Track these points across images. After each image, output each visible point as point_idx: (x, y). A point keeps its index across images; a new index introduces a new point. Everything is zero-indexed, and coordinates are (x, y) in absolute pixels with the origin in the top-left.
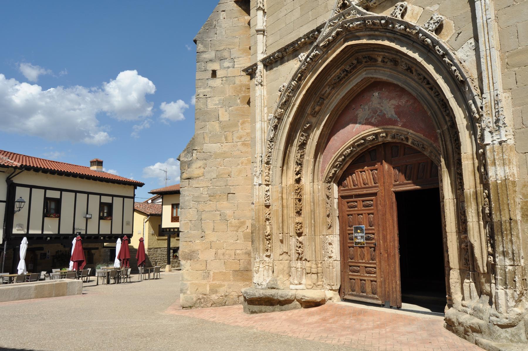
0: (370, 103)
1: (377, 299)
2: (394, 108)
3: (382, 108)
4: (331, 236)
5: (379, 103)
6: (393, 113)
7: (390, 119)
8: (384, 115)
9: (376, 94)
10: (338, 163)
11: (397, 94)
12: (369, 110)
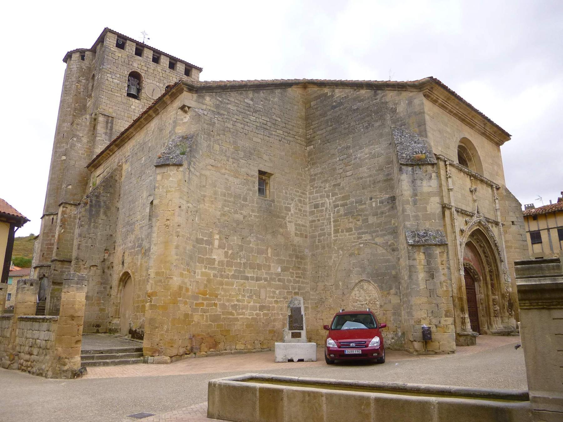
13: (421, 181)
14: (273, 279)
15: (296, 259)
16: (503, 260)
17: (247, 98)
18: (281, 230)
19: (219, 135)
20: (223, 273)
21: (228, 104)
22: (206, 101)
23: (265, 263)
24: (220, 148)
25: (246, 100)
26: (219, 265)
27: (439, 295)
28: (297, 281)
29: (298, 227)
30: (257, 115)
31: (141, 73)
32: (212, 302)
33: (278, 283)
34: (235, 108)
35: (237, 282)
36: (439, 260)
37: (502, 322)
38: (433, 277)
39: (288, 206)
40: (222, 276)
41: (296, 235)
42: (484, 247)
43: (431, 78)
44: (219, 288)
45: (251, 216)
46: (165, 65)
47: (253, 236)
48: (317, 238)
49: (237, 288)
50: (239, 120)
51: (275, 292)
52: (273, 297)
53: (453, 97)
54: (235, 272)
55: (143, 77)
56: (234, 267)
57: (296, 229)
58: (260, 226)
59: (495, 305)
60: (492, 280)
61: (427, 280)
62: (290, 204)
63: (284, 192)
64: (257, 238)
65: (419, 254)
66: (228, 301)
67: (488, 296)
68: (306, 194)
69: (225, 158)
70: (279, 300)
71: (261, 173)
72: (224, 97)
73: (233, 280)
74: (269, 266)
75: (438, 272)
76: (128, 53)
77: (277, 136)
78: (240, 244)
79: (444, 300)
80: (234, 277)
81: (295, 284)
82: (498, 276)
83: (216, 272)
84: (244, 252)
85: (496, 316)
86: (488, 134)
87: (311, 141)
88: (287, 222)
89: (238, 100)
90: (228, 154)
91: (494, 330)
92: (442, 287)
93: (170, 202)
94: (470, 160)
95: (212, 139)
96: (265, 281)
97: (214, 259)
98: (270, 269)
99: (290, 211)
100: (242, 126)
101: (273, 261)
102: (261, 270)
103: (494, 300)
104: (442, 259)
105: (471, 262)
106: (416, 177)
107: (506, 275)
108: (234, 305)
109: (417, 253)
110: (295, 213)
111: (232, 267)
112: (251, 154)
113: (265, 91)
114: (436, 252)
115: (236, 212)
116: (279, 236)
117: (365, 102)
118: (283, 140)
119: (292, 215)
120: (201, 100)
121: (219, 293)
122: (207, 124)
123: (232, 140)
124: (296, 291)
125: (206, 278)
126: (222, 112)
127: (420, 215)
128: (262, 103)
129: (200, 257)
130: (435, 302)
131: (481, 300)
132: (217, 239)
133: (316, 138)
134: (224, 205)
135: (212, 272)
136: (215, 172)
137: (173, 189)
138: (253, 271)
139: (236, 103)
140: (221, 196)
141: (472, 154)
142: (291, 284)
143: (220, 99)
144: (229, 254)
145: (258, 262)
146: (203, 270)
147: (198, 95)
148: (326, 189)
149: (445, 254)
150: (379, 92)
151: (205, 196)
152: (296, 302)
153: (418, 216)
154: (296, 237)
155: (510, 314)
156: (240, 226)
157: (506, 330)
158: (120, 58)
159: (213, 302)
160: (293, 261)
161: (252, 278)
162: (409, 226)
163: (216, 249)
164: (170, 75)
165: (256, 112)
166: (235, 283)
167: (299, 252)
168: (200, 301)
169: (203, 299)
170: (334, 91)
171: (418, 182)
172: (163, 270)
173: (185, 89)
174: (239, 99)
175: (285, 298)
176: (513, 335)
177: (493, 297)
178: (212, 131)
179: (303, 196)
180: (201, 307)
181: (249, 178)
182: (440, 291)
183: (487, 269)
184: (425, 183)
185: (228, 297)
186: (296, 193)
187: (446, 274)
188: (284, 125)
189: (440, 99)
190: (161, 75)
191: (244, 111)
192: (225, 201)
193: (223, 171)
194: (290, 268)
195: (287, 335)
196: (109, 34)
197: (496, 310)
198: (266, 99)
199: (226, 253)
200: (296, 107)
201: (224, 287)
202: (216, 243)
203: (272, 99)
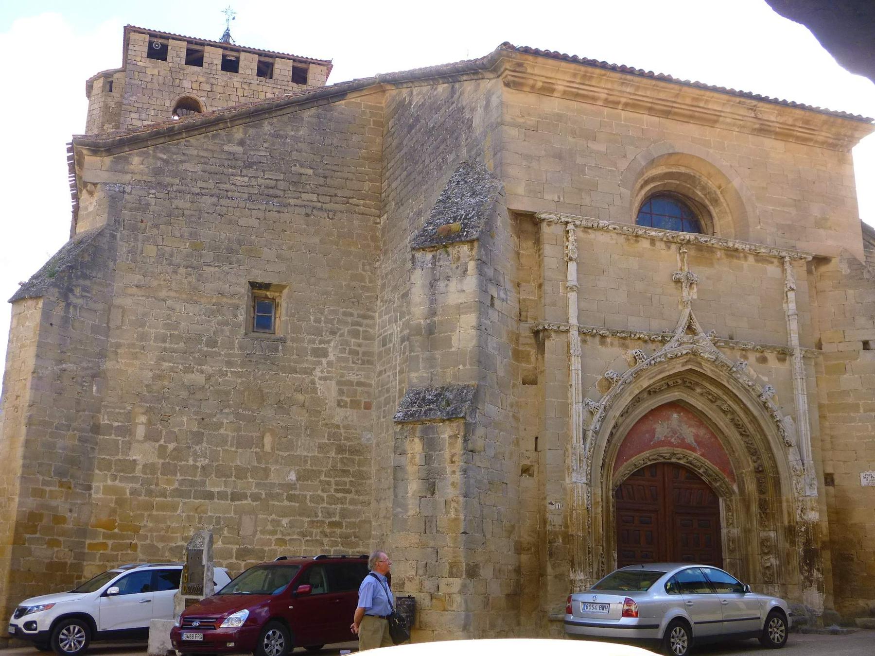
0: (670, 422)
5: (678, 426)
6: (693, 442)
8: (684, 439)
9: (675, 416)
10: (627, 472)
12: (668, 428)
13: (446, 282)
14: (277, 497)
15: (336, 453)
17: (229, 141)
18: (300, 397)
19: (156, 226)
20: (153, 487)
21: (182, 162)
22: (131, 167)
23: (256, 464)
24: (158, 250)
25: (225, 148)
26: (144, 473)
27: (440, 529)
28: (339, 499)
29: (345, 388)
30: (251, 172)
31: (198, 98)
32: (125, 541)
33: (286, 503)
34: (198, 168)
35: (184, 503)
36: (447, 454)
38: (434, 490)
39: (323, 345)
40: (149, 493)
41: (339, 403)
42: (733, 412)
43: (506, 44)
44: (142, 515)
45: (223, 374)
46: (248, 72)
47: (228, 414)
48: (383, 409)
49: (184, 514)
50: (207, 189)
51: (279, 521)
52: (274, 533)
53: (598, 71)
54: (180, 485)
55: (203, 104)
56: (178, 474)
57: (341, 392)
58: (246, 394)
59: (766, 554)
60: (761, 491)
61: (421, 497)
62: (329, 342)
63: (312, 318)
64: (238, 416)
65: (413, 440)
66: (162, 539)
67: (747, 531)
68: (372, 318)
69: (170, 269)
70: (287, 538)
71: (253, 285)
72: (174, 149)
73: (176, 499)
74: (266, 471)
75: (443, 479)
76: (170, 65)
77: (304, 206)
78: (196, 429)
79: (449, 541)
80: (179, 493)
81: (333, 506)
82: (777, 483)
83: (138, 486)
84: (204, 444)
85: (766, 582)
86: (778, 130)
87: (385, 206)
88: (317, 380)
89: (206, 150)
90: (176, 260)
92: (447, 512)
93: (23, 364)
94: (715, 201)
95: (140, 237)
96: (253, 501)
97: (135, 460)
98: (267, 476)
99: (325, 355)
100: (214, 200)
101: (277, 461)
102: (246, 478)
103: (764, 542)
104: (453, 451)
105: (693, 450)
106: (438, 274)
108: (177, 547)
109: (408, 439)
110: (339, 359)
111: (175, 475)
112: (231, 251)
113: (275, 120)
114: (442, 436)
115: (188, 370)
116: (294, 408)
117: (442, 111)
118: (315, 212)
119: (330, 364)
120: (119, 167)
121: (142, 525)
122: (131, 210)
123: (186, 231)
124: (334, 519)
125: (114, 497)
126: (168, 180)
127: (437, 356)
128: (265, 145)
129: (103, 459)
130: (432, 543)
131: (729, 540)
132: (142, 423)
133: (391, 198)
134: (162, 359)
135: (128, 487)
136: (144, 298)
137: (28, 342)
138: (226, 483)
139: (202, 157)
140: (155, 342)
141: (720, 187)
142: (321, 506)
143: (165, 157)
144: (168, 451)
145: (239, 463)
146: (109, 482)
147: (115, 158)
148: (395, 305)
149: (460, 440)
150: (457, 85)
151: (118, 346)
152: (199, 541)
153: (435, 359)
154: (338, 410)
155: (806, 578)
156: (199, 396)
158: (155, 77)
159: (128, 541)
160: (329, 457)
161: (222, 496)
162: (415, 381)
163: (138, 441)
164: (260, 88)
165: (249, 166)
166: (181, 504)
167: (347, 439)
168: (100, 540)
169: (106, 536)
170: (411, 94)
171: (441, 284)
172: (5, 486)
173: (85, 152)
174: (210, 147)
175: (303, 534)
177: (763, 534)
178: (142, 221)
179: (365, 322)
180: (101, 552)
181: (225, 300)
182: (443, 521)
183: (748, 467)
184: (453, 285)
185: (163, 533)
186: (344, 318)
187: (457, 483)
188: (321, 181)
189: (559, 82)
190: (240, 92)
191: (222, 169)
192: (165, 349)
193: (163, 293)
194: (322, 471)
195: (179, 604)
196: (134, 36)
198: (278, 136)
199: (163, 448)
200: (355, 138)
201: (154, 513)
202: (140, 432)
203: (293, 133)
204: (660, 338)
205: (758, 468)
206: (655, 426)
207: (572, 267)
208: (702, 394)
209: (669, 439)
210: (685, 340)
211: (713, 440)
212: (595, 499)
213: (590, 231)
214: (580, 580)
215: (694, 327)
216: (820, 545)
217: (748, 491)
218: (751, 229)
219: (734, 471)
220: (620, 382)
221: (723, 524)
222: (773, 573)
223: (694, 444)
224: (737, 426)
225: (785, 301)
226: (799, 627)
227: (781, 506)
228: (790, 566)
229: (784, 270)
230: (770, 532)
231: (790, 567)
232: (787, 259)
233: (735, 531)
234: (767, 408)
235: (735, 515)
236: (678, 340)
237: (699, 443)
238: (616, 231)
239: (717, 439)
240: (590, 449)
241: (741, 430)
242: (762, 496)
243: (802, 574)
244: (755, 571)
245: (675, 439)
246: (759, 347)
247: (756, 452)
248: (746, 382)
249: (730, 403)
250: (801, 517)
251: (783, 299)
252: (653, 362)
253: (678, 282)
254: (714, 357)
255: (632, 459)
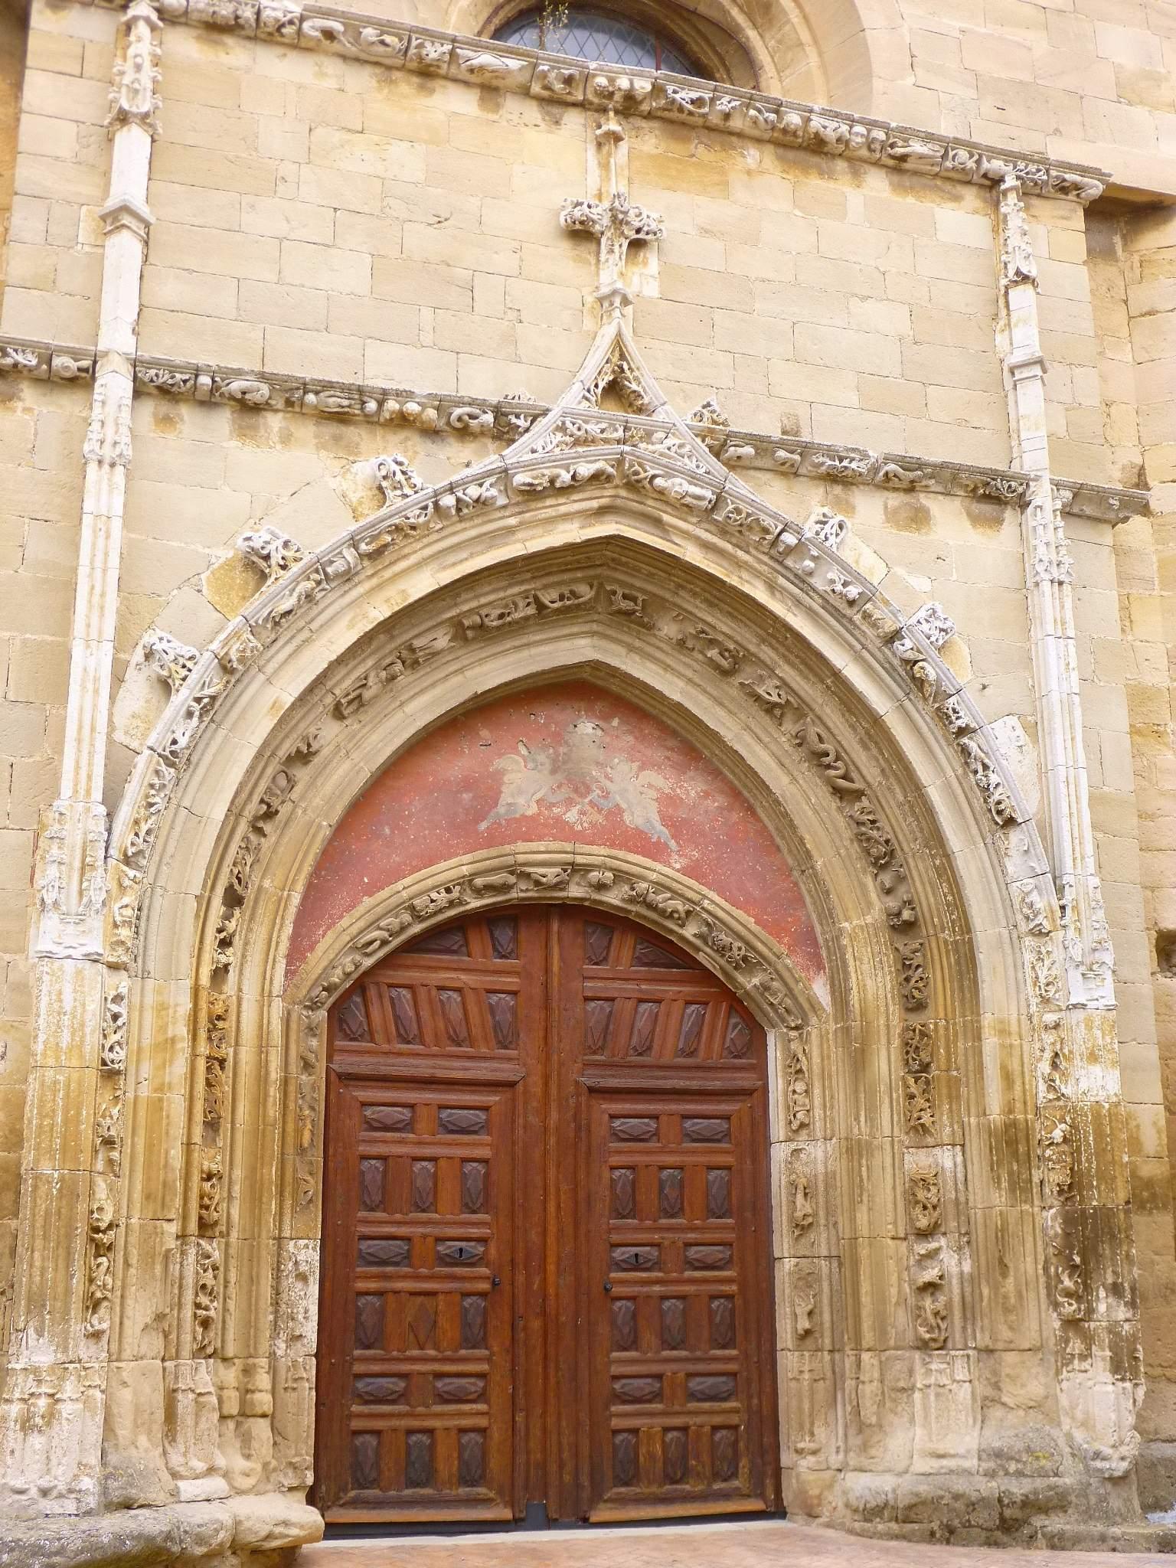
0: (562, 750)
1: (485, 1502)
2: (656, 800)
3: (608, 783)
4: (302, 1242)
6: (655, 818)
7: (639, 833)
8: (618, 811)
10: (376, 934)
11: (668, 758)
16: (1025, 803)
37: (986, 1404)
42: (799, 709)
59: (924, 1234)
60: (915, 1005)
67: (855, 1150)
85: (924, 1346)
91: (862, 1485)
105: (655, 851)
107: (1053, 946)
155: (1072, 1324)
157: (989, 1488)
176: (1057, 1543)
177: (917, 1161)
197: (931, 1287)
204: (488, 418)
205: (899, 914)
206: (500, 763)
207: (133, 143)
208: (681, 644)
209: (556, 810)
210: (593, 428)
211: (735, 816)
212: (163, 1028)
213: (229, 40)
214: (34, 1371)
215: (634, 386)
216: (1122, 1195)
217: (863, 1001)
218: (878, 85)
219: (818, 929)
220: (295, 568)
221: (778, 1128)
222: (949, 1305)
223: (660, 831)
224: (818, 758)
225: (1002, 323)
226: (1038, 1521)
227: (979, 1053)
228: (1011, 1280)
229: (999, 224)
230: (937, 1151)
231: (1010, 1284)
232: (1010, 181)
233: (818, 1155)
234: (920, 683)
235: (817, 1091)
236: (562, 428)
237: (676, 827)
238: (335, 46)
239: (754, 813)
240: (136, 822)
241: (832, 772)
242: (916, 1020)
243: (1056, 1305)
244: (881, 1299)
245: (583, 813)
246: (892, 467)
247: (892, 854)
248: (839, 587)
249: (786, 672)
250: (1051, 1088)
251: (995, 317)
252: (448, 501)
253: (581, 233)
254: (708, 494)
255: (399, 885)
